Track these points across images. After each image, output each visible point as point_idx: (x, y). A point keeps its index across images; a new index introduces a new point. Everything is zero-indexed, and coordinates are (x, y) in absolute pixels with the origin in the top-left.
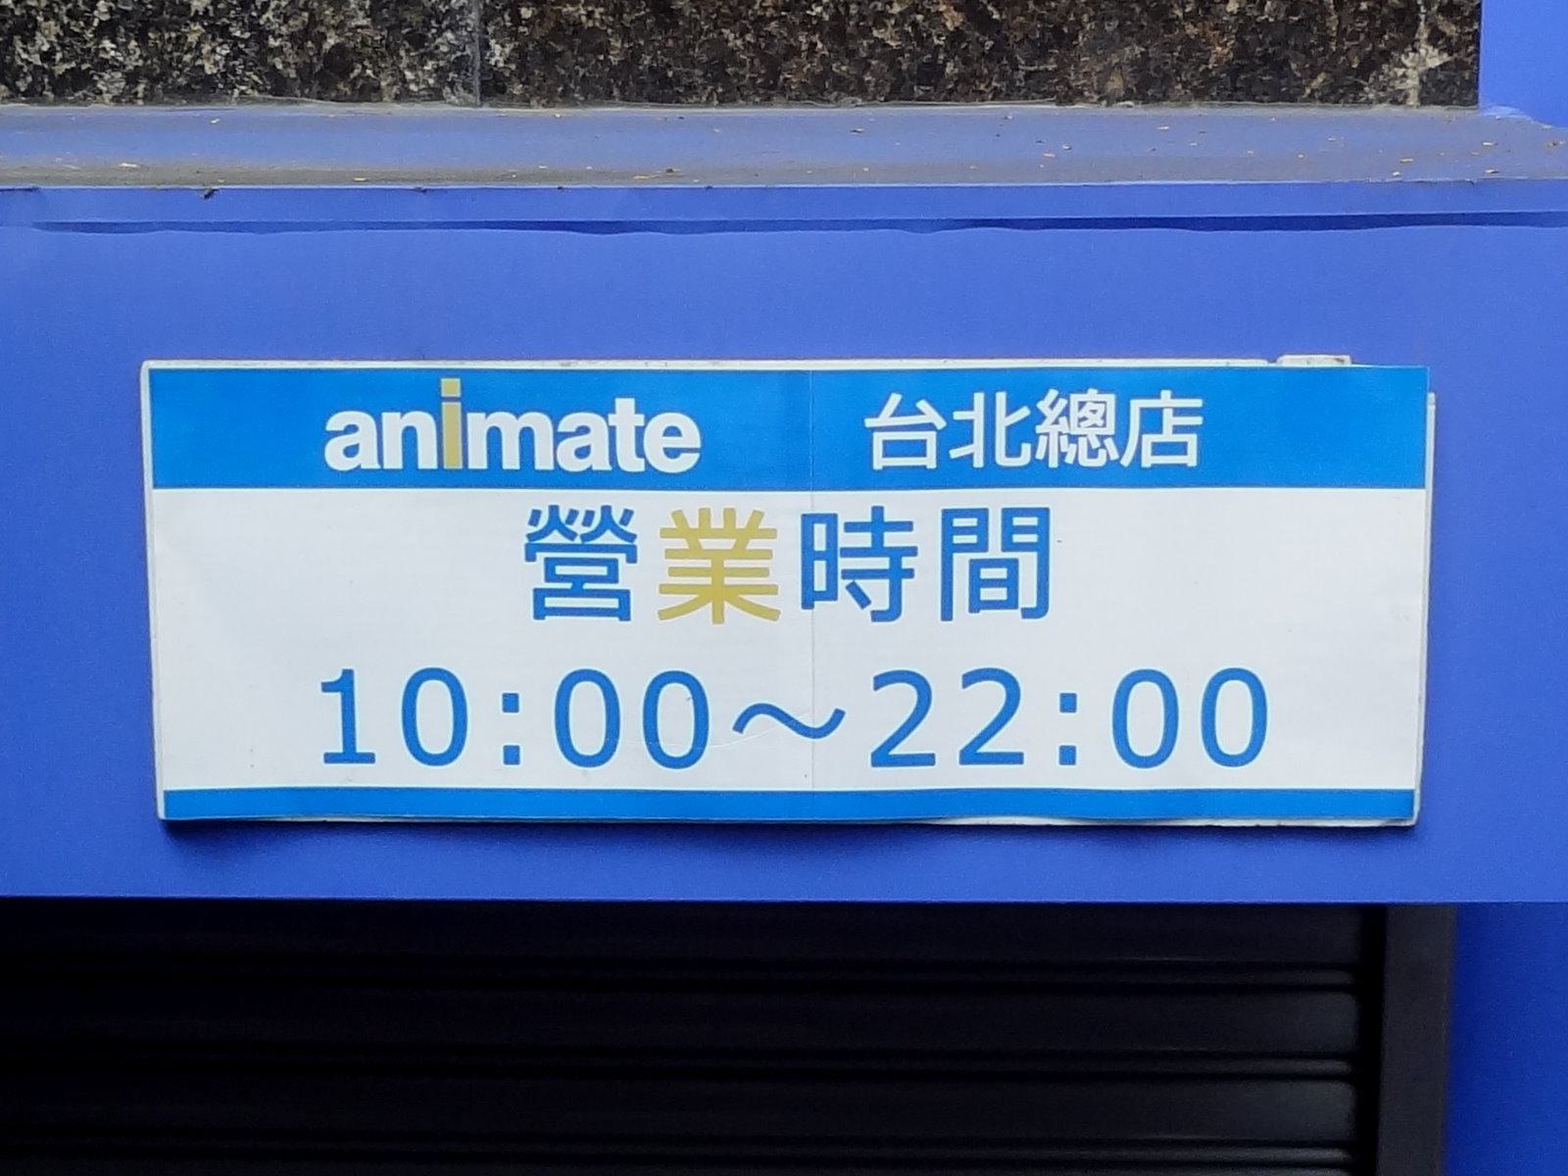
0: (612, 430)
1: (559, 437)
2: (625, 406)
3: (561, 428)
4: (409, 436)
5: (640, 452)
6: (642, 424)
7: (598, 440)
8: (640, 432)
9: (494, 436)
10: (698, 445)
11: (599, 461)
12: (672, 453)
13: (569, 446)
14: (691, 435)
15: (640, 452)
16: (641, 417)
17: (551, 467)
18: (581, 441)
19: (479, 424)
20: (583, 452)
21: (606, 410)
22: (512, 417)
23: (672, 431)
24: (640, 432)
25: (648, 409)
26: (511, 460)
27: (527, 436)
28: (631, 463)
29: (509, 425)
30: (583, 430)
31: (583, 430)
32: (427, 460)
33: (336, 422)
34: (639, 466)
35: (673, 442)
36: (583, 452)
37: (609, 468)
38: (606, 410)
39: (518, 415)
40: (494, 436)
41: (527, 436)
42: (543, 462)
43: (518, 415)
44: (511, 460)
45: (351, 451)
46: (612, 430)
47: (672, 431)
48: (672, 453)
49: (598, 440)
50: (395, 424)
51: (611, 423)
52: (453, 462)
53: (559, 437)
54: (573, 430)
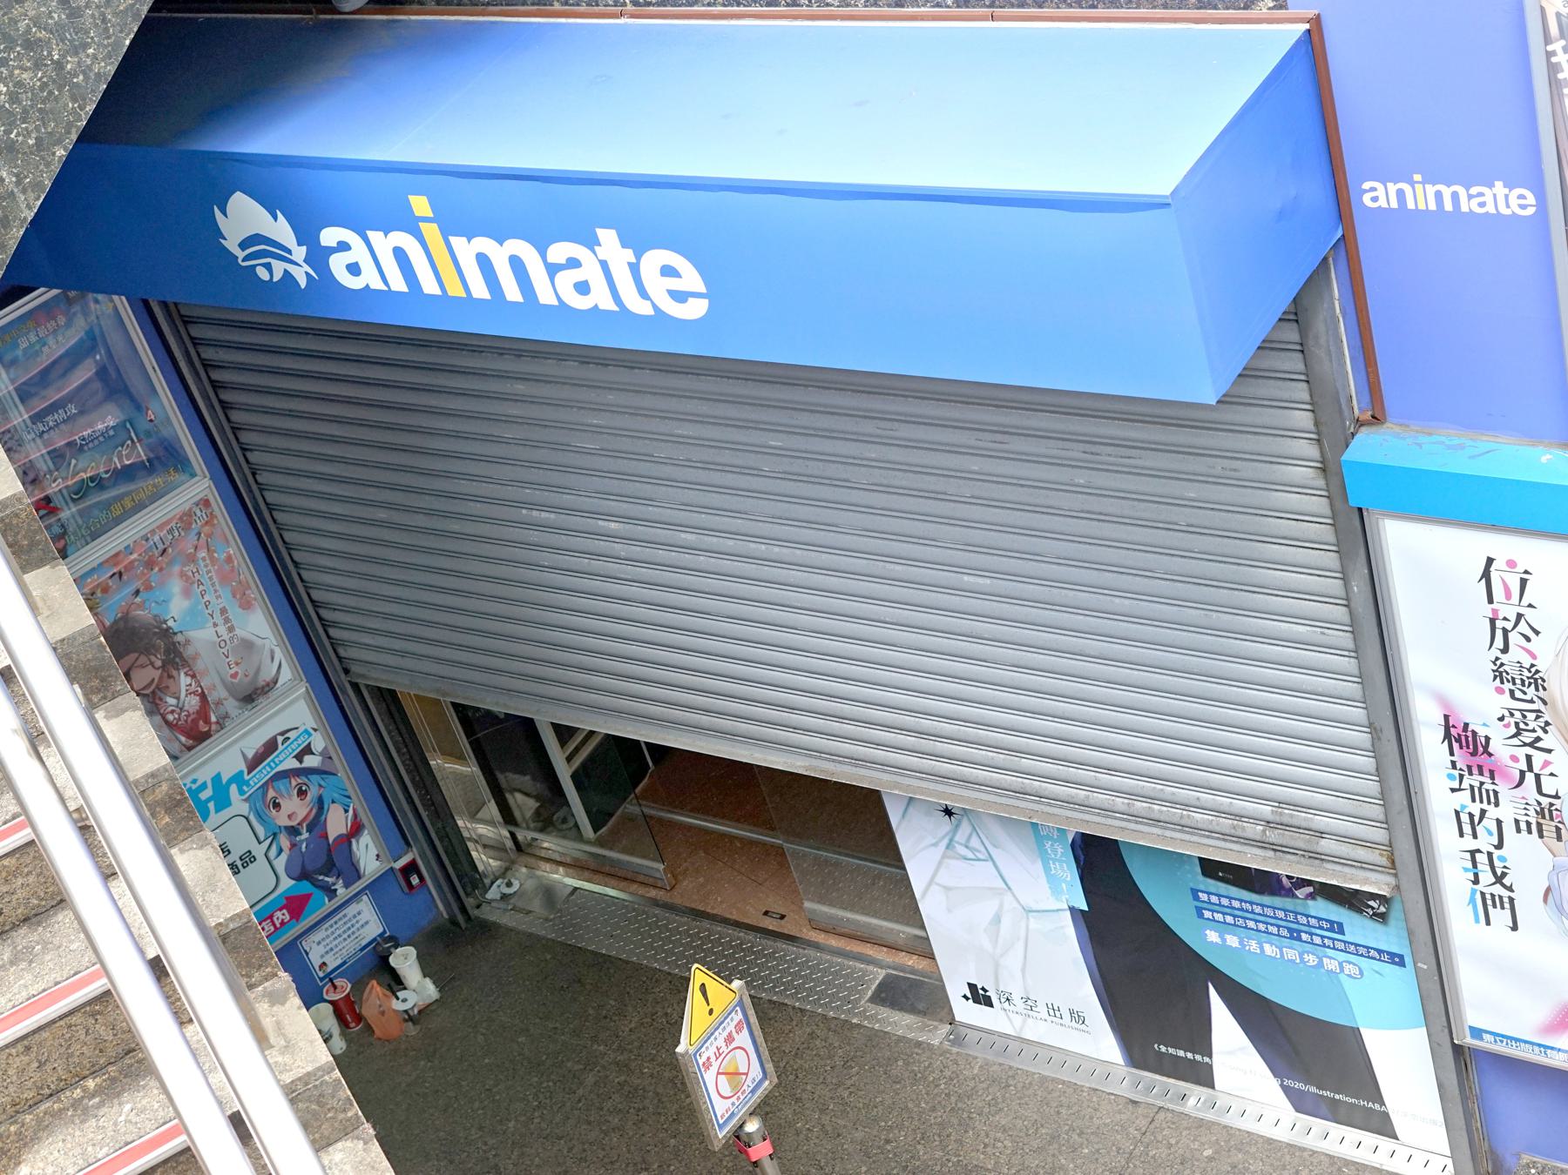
0: (1495, 196)
1: (1470, 197)
2: (1499, 184)
4: (1400, 193)
5: (1508, 206)
7: (1488, 198)
8: (1507, 196)
9: (1439, 195)
10: (1534, 203)
11: (1490, 208)
12: (1523, 207)
13: (1475, 202)
14: (1531, 199)
15: (1508, 206)
19: (1431, 190)
21: (1491, 186)
23: (1521, 197)
24: (1507, 196)
25: (1510, 185)
26: (1448, 206)
27: (1455, 196)
28: (1504, 211)
29: (1447, 192)
30: (1481, 194)
31: (1481, 194)
32: (1411, 205)
33: (1366, 185)
34: (1507, 212)
35: (1522, 202)
36: (1482, 205)
38: (1491, 186)
40: (1439, 195)
41: (1455, 196)
42: (1464, 208)
44: (1448, 206)
45: (1375, 199)
46: (1495, 196)
47: (1521, 197)
48: (1523, 207)
49: (1488, 198)
50: (1392, 188)
53: (1470, 197)
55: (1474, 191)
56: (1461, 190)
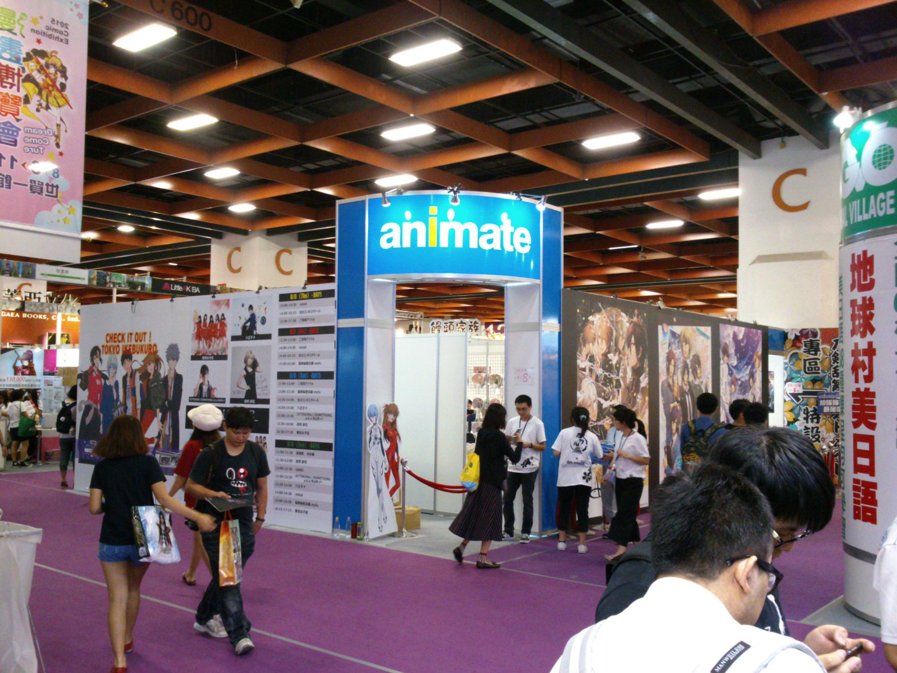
0: (502, 232)
1: (480, 234)
3: (481, 230)
5: (512, 244)
6: (513, 231)
7: (496, 236)
8: (512, 234)
15: (512, 244)
16: (513, 228)
17: (476, 247)
18: (489, 236)
19: (445, 227)
20: (490, 241)
21: (499, 223)
22: (460, 224)
24: (512, 234)
27: (466, 234)
28: (508, 248)
30: (490, 232)
31: (490, 232)
32: (421, 243)
34: (511, 249)
37: (500, 249)
38: (499, 223)
39: (463, 224)
41: (466, 234)
42: (473, 245)
43: (463, 224)
44: (459, 244)
46: (502, 232)
49: (496, 236)
51: (502, 229)
52: (433, 244)
53: (480, 234)
54: (486, 231)
55: (485, 228)
56: (472, 227)
